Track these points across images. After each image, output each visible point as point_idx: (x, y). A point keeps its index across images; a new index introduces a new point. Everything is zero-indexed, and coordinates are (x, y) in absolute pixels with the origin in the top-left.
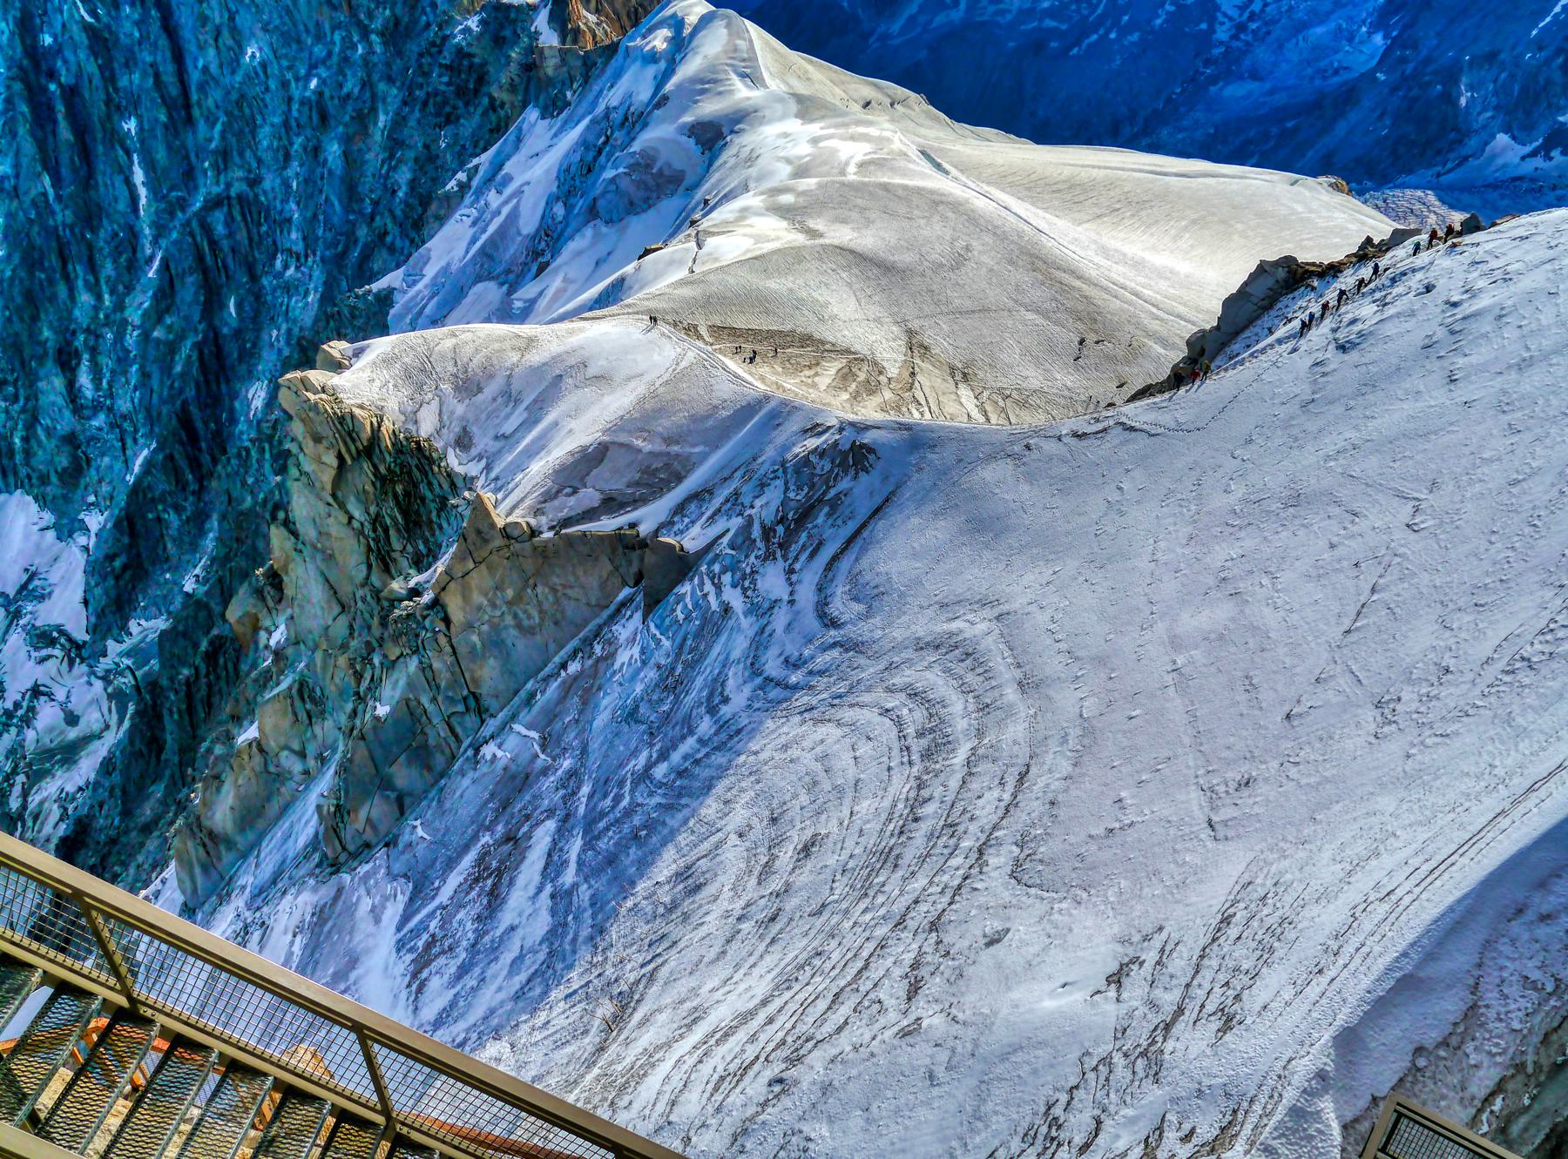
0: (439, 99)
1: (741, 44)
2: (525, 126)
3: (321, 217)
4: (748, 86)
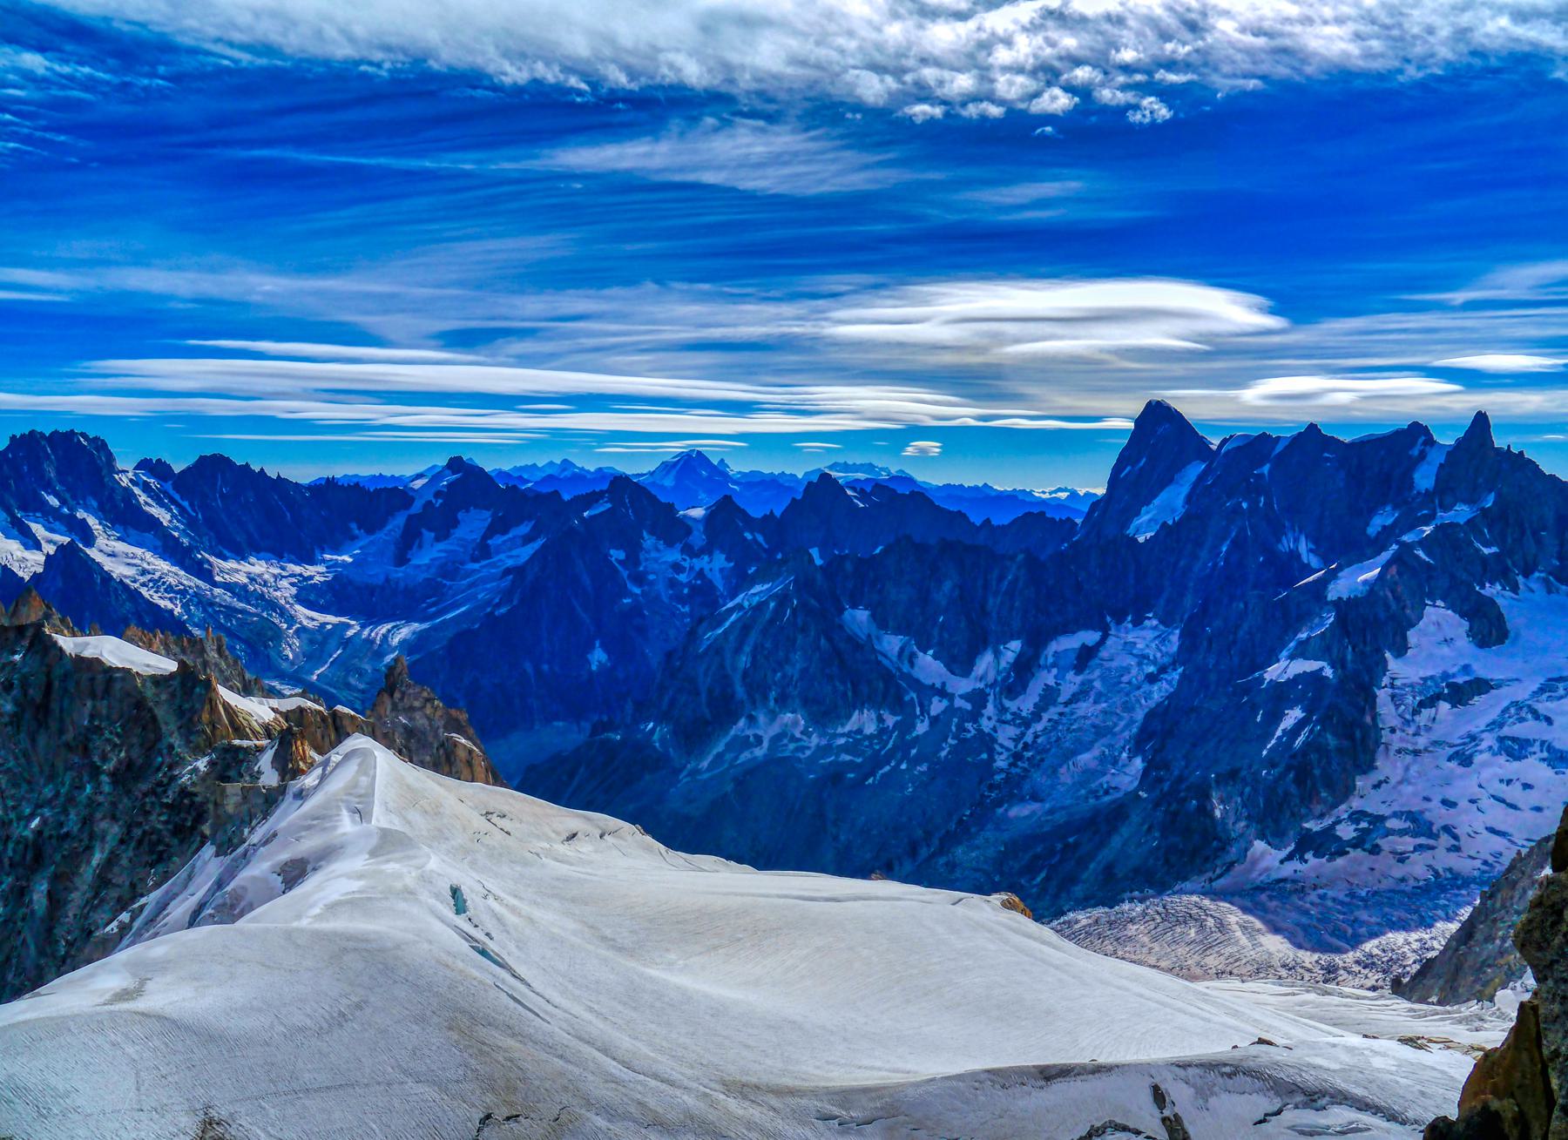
0: (154, 837)
1: (364, 780)
2: (199, 864)
3: (14, 961)
4: (353, 821)
